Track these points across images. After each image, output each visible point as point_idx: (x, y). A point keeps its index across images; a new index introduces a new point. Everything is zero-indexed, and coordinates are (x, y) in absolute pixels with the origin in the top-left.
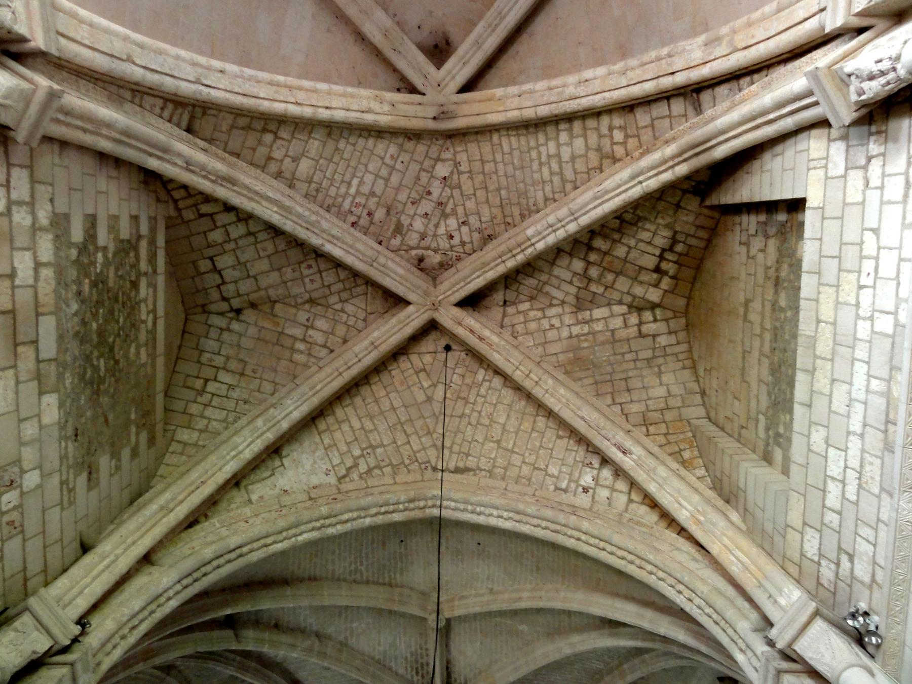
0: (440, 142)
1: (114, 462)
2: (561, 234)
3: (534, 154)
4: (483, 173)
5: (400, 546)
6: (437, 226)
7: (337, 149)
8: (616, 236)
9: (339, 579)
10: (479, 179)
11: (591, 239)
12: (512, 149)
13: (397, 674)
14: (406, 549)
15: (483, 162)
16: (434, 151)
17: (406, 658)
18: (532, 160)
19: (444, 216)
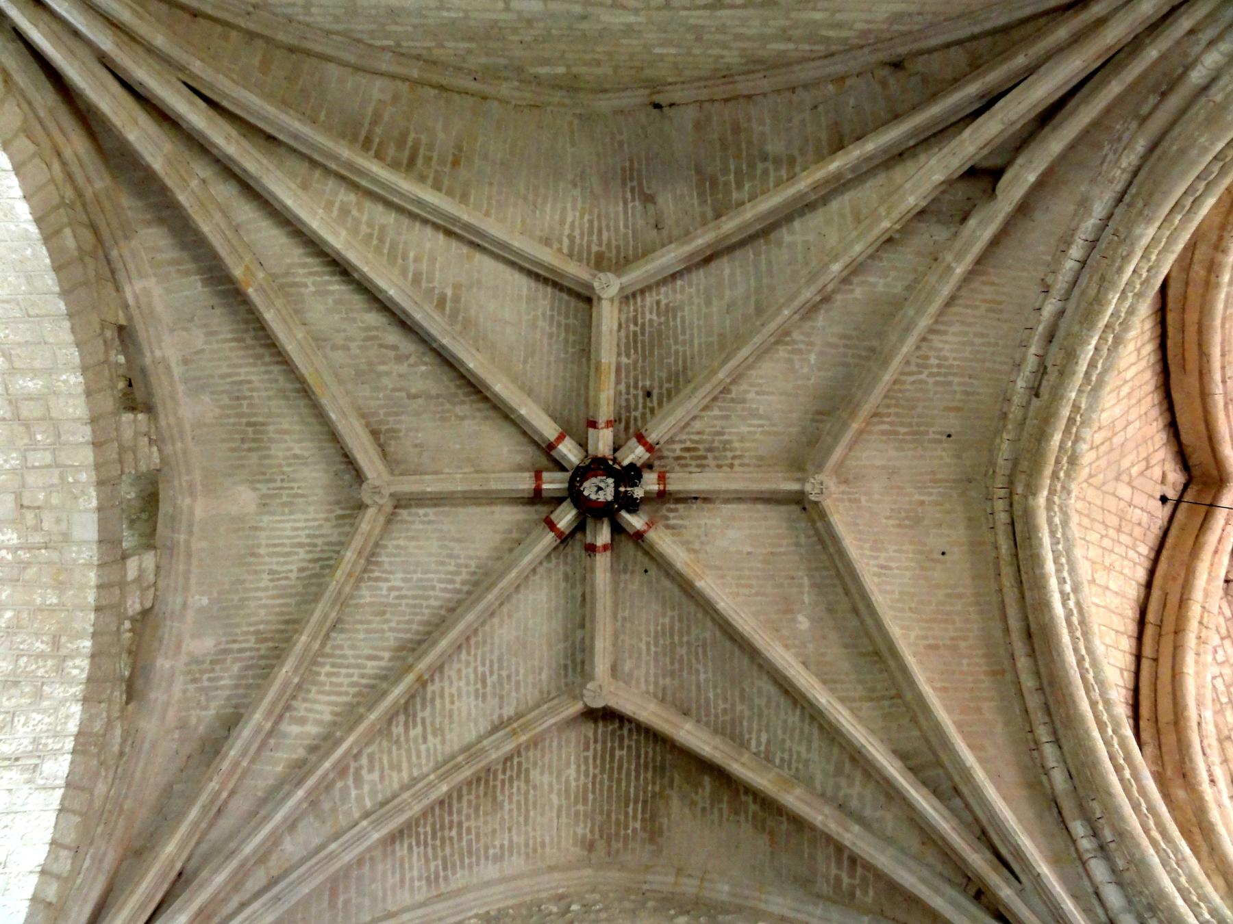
5: (941, 433)
13: (694, 418)
14: (930, 441)
17: (721, 433)
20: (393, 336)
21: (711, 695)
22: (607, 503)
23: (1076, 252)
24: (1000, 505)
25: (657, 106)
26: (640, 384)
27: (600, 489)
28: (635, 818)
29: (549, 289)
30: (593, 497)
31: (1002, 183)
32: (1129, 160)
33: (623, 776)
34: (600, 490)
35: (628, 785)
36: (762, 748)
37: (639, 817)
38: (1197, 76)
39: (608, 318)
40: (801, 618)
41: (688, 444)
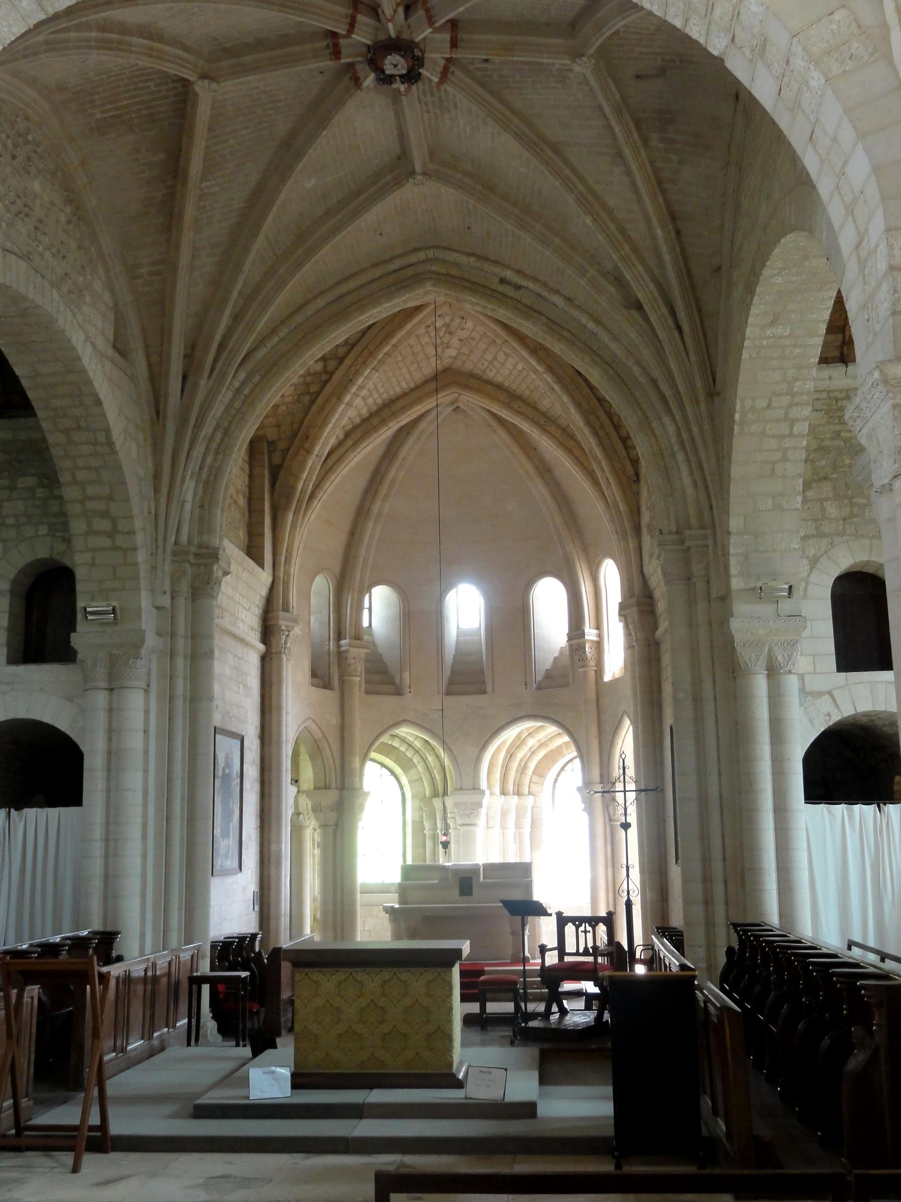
0: (453, 367)
2: (354, 390)
3: (382, 390)
4: (418, 362)
6: (452, 320)
7: (531, 391)
8: (309, 379)
10: (421, 356)
11: (325, 367)
12: (399, 385)
15: (420, 368)
16: (458, 364)
18: (383, 386)
19: (447, 326)
21: (231, 142)
24: (421, 256)
28: (102, 112)
30: (387, 62)
31: (633, 312)
33: (133, 93)
34: (394, 64)
35: (126, 99)
36: (206, 191)
37: (106, 115)
38: (666, 420)
40: (313, 182)
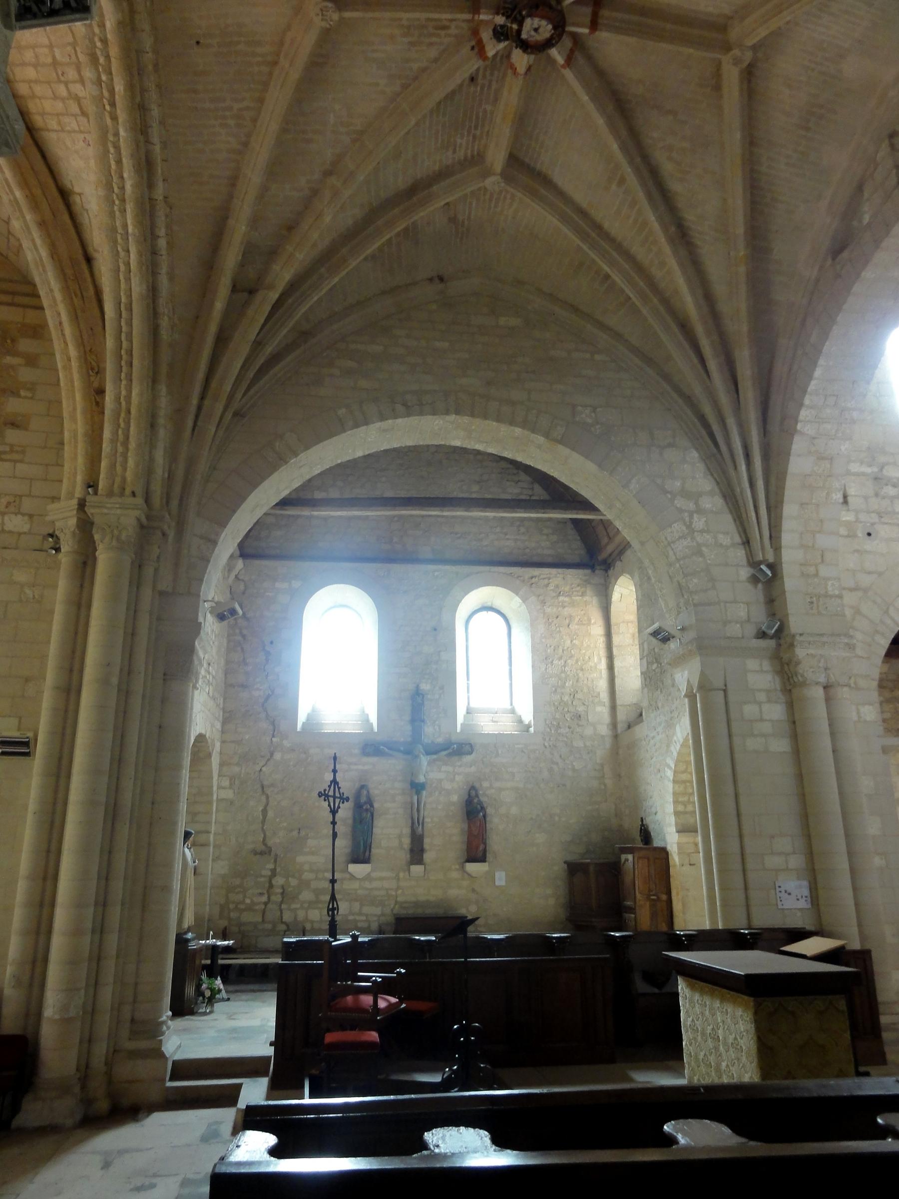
1: (22, 393)
9: (246, 144)
13: (436, 60)
17: (412, 44)
20: (667, 168)
22: (530, 15)
23: (162, 243)
25: (441, 279)
26: (479, 88)
27: (536, 30)
29: (538, 167)
32: (164, 322)
39: (497, 157)
41: (443, 33)
